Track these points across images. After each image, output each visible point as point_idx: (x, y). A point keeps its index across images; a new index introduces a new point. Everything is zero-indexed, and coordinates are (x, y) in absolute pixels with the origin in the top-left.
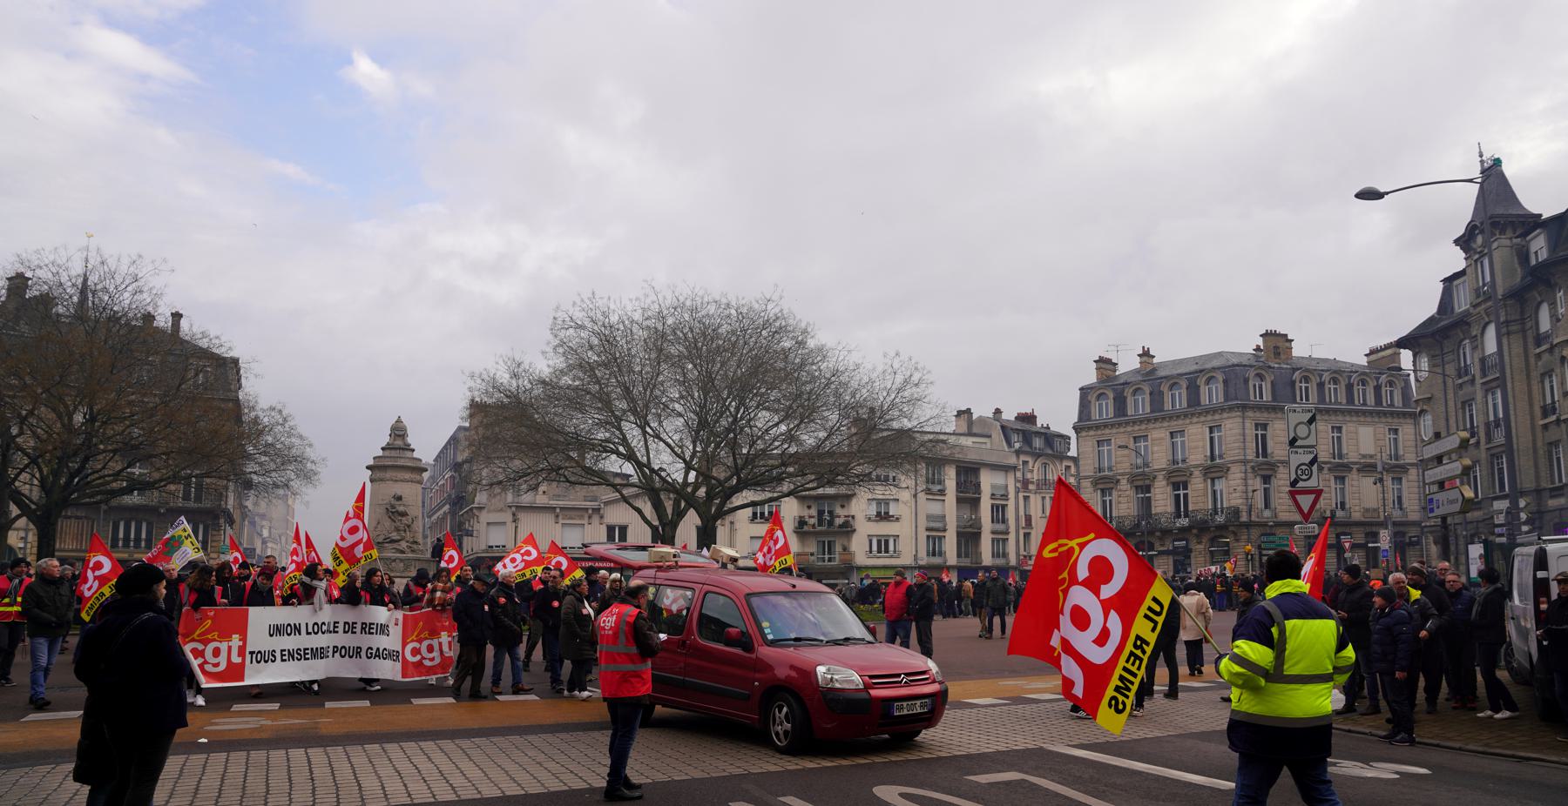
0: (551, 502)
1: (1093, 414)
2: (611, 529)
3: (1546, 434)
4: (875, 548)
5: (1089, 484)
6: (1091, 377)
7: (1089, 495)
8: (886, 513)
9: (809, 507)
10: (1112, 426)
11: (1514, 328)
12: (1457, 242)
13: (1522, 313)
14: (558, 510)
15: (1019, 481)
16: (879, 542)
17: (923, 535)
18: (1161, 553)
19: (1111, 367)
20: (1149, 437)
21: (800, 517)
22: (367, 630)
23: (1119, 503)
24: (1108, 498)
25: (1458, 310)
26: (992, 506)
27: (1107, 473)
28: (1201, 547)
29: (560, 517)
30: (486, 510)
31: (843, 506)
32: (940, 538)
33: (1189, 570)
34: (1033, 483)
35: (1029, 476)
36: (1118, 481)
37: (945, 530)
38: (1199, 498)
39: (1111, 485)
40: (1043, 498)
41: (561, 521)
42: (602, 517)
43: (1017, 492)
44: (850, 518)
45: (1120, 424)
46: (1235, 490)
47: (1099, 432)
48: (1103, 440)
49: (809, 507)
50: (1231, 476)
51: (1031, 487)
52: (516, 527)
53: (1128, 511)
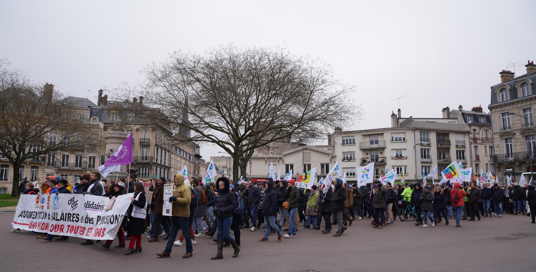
1: (498, 99)
2: (287, 166)
5: (498, 137)
6: (498, 80)
7: (498, 142)
8: (401, 155)
9: (367, 154)
10: (509, 104)
14: (266, 159)
15: (471, 139)
17: (419, 165)
19: (511, 75)
20: (532, 108)
21: (362, 158)
22: (71, 218)
23: (516, 145)
24: (509, 144)
26: (457, 151)
27: (508, 130)
29: (267, 162)
31: (381, 153)
32: (429, 167)
34: (479, 139)
35: (477, 136)
36: (514, 134)
37: (431, 163)
39: (511, 136)
40: (486, 147)
41: (268, 163)
42: (283, 161)
43: (471, 144)
44: (384, 158)
45: (514, 103)
47: (502, 109)
48: (505, 113)
49: (367, 154)
51: (478, 141)
52: (251, 166)
53: (522, 150)
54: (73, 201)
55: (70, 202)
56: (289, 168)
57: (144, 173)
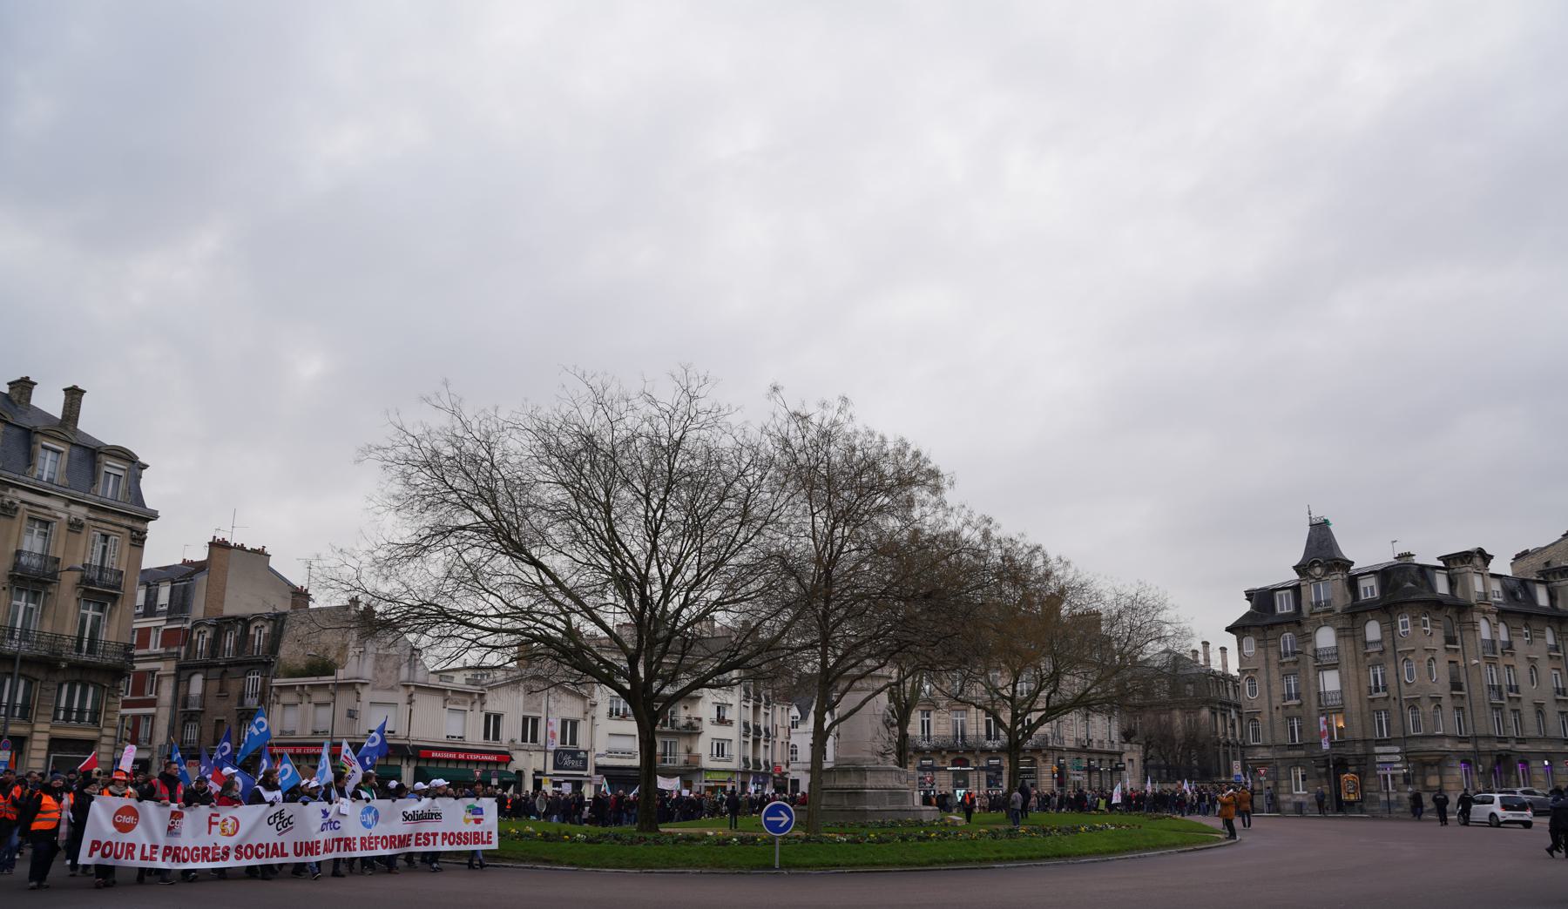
0: (441, 683)
2: (487, 717)
3: (1372, 704)
4: (715, 752)
11: (1347, 633)
12: (1294, 567)
13: (1352, 625)
14: (450, 693)
16: (718, 745)
25: (1279, 611)
30: (370, 686)
31: (686, 708)
52: (411, 711)
54: (281, 818)
55: (272, 820)
56: (493, 723)
57: (76, 705)
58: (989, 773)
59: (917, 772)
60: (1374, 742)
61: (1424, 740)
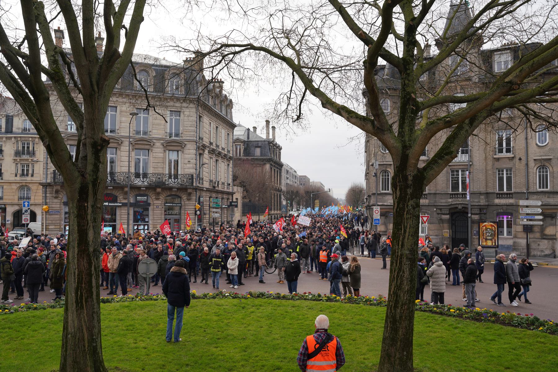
18: (124, 205)
28: (159, 202)
33: (147, 220)
38: (159, 164)
46: (189, 161)
50: (186, 151)
58: (136, 209)
59: (63, 207)
60: (495, 195)
61: (551, 196)
